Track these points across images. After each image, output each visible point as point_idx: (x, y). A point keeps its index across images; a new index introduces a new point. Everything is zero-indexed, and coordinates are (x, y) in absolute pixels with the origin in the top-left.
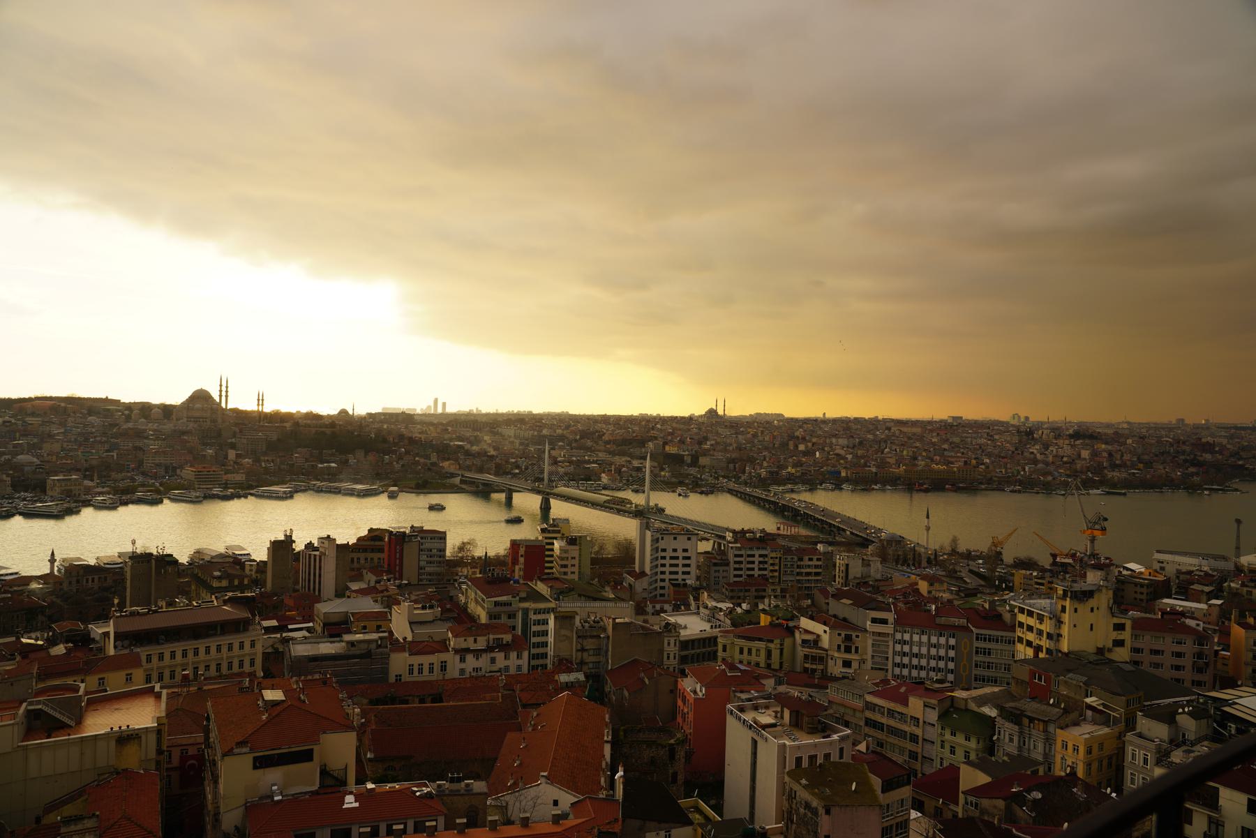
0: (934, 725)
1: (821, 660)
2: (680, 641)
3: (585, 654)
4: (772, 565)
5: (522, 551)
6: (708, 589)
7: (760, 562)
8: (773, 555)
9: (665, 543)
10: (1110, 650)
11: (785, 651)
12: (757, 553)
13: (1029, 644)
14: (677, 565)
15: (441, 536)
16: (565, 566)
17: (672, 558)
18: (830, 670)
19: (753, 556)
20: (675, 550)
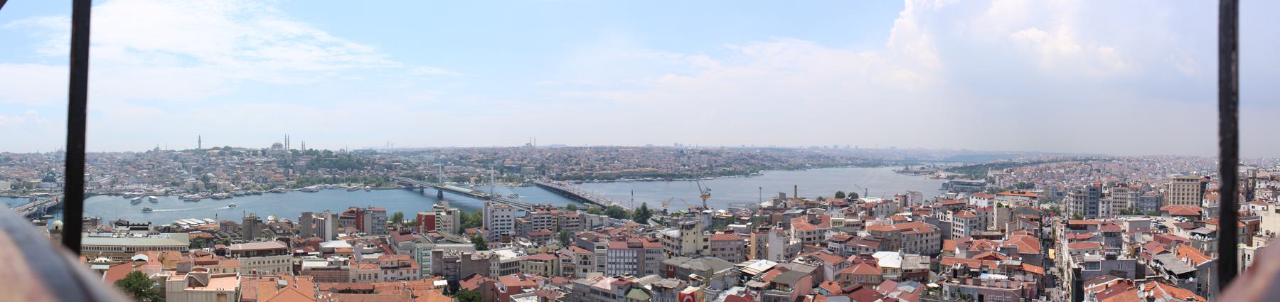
0: (622, 297)
1: (572, 269)
2: (501, 264)
3: (449, 271)
4: (554, 222)
5: (423, 218)
6: (521, 235)
7: (548, 221)
8: (554, 217)
9: (499, 213)
10: (702, 251)
11: (554, 266)
12: (545, 216)
13: (668, 252)
14: (504, 224)
15: (384, 212)
16: (446, 226)
17: (501, 221)
18: (577, 274)
19: (543, 218)
20: (503, 216)
